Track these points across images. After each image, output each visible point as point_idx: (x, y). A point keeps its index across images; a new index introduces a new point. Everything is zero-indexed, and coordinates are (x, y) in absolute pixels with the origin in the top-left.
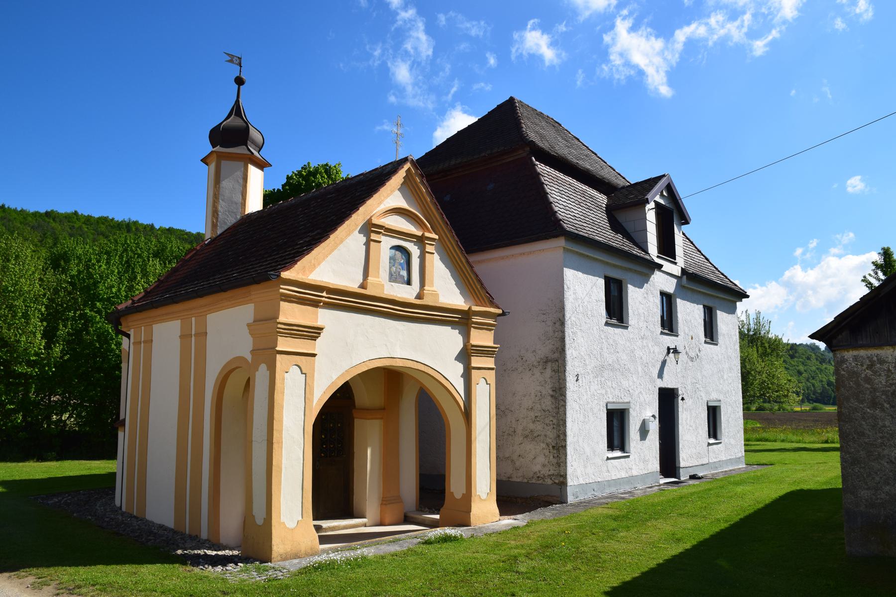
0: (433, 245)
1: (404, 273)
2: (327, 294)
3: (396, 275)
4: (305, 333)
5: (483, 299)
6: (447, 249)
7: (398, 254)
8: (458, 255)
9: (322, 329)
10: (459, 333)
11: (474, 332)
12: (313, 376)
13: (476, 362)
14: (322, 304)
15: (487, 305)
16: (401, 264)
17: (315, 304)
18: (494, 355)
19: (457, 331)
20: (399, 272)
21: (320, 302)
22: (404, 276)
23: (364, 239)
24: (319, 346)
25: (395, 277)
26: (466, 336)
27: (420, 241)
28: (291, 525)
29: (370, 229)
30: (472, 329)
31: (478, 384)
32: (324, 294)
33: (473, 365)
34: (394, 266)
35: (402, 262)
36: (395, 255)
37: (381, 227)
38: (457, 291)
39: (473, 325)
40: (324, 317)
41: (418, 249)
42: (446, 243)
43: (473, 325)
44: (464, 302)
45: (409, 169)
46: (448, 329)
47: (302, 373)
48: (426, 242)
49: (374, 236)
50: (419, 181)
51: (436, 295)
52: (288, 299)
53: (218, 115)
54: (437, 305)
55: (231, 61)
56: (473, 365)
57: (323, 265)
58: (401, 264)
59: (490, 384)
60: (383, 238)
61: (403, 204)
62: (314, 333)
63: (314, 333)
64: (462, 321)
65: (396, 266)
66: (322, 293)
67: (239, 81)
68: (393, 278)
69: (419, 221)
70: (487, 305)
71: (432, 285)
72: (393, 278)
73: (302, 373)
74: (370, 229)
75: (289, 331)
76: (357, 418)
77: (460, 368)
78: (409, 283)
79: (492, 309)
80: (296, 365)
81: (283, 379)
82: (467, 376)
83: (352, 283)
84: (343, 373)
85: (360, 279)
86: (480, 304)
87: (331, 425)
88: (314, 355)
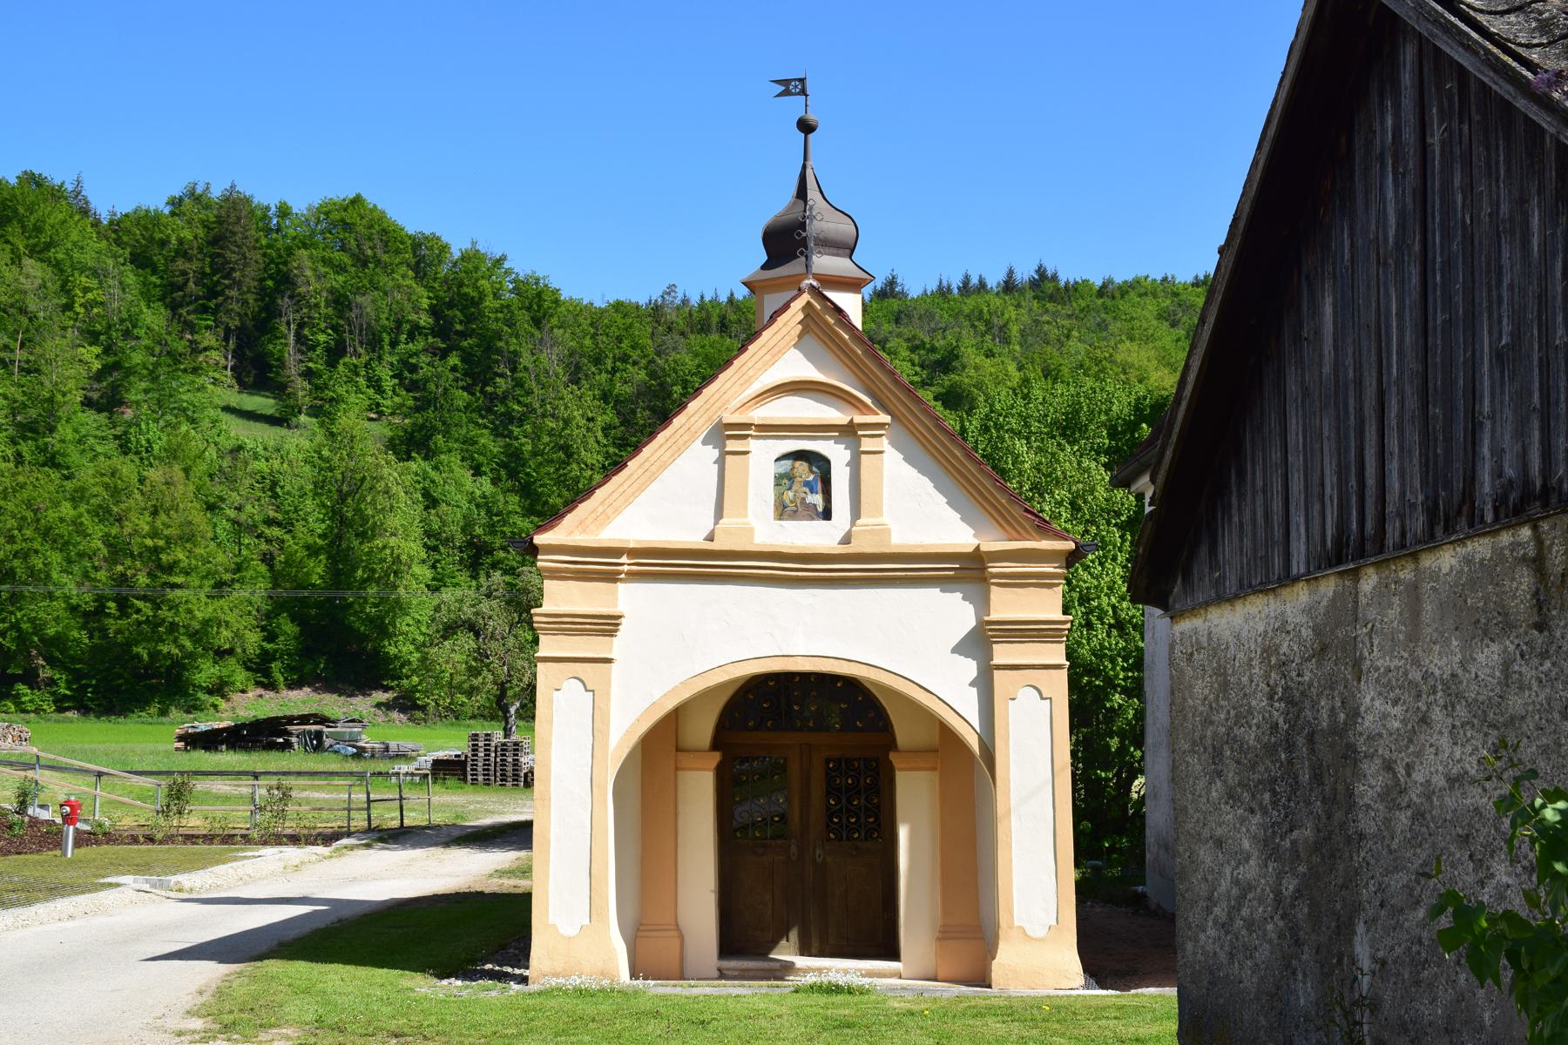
0: (880, 436)
1: (817, 499)
2: (628, 558)
3: (796, 506)
4: (588, 626)
5: (1024, 528)
6: (920, 437)
7: (802, 467)
8: (941, 442)
9: (620, 617)
10: (964, 599)
11: (996, 593)
12: (608, 694)
13: (1003, 653)
14: (623, 576)
15: (1031, 534)
16: (807, 484)
17: (611, 577)
18: (1062, 637)
19: (959, 595)
20: (804, 499)
21: (620, 573)
22: (815, 505)
23: (716, 453)
24: (616, 647)
25: (795, 508)
26: (983, 604)
27: (848, 433)
28: (569, 930)
29: (725, 434)
30: (993, 588)
31: (1014, 699)
32: (624, 559)
33: (997, 661)
34: (790, 489)
35: (811, 477)
36: (793, 468)
37: (747, 426)
38: (955, 516)
39: (992, 581)
40: (628, 598)
41: (845, 449)
42: (914, 425)
43: (992, 581)
44: (975, 536)
45: (808, 303)
46: (934, 593)
47: (586, 690)
48: (860, 433)
49: (732, 445)
50: (833, 322)
51: (885, 532)
52: (556, 575)
53: (776, 203)
54: (887, 551)
55: (786, 93)
56: (997, 661)
57: (628, 512)
58: (807, 484)
59: (1051, 699)
60: (753, 445)
61: (803, 369)
62: (607, 625)
63: (607, 625)
64: (961, 574)
65: (794, 488)
66: (620, 558)
67: (806, 127)
68: (783, 511)
69: (843, 395)
70: (1031, 534)
71: (878, 511)
72: (783, 511)
73: (586, 690)
74: (725, 434)
75: (557, 626)
76: (901, 769)
77: (969, 668)
78: (827, 514)
79: (1044, 542)
80: (575, 678)
81: (551, 701)
82: (985, 684)
83: (690, 536)
84: (676, 687)
85: (708, 523)
86: (1018, 537)
87: (850, 782)
88: (609, 661)
